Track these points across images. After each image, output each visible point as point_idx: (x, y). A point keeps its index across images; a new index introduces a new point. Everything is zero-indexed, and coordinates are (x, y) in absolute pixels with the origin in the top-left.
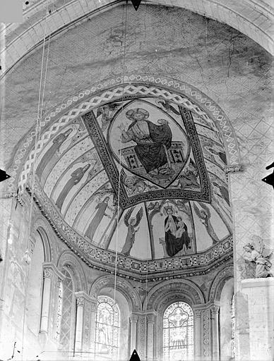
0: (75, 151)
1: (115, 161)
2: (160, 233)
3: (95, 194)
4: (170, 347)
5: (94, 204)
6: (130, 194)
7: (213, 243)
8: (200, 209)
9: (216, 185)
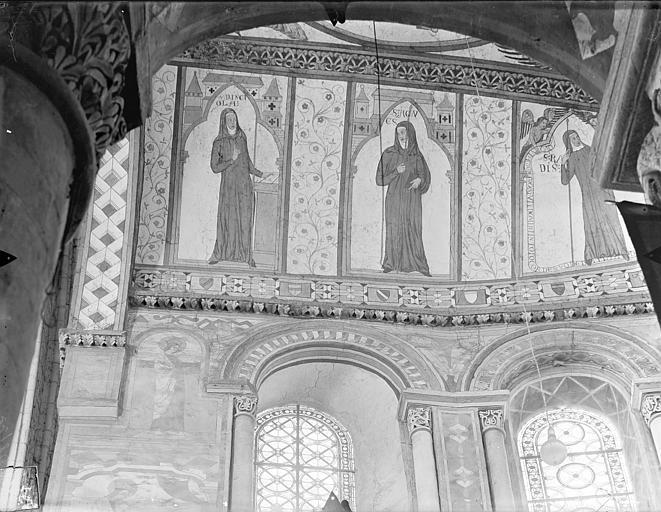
0: (313, 137)
1: (457, 53)
3: (518, 158)
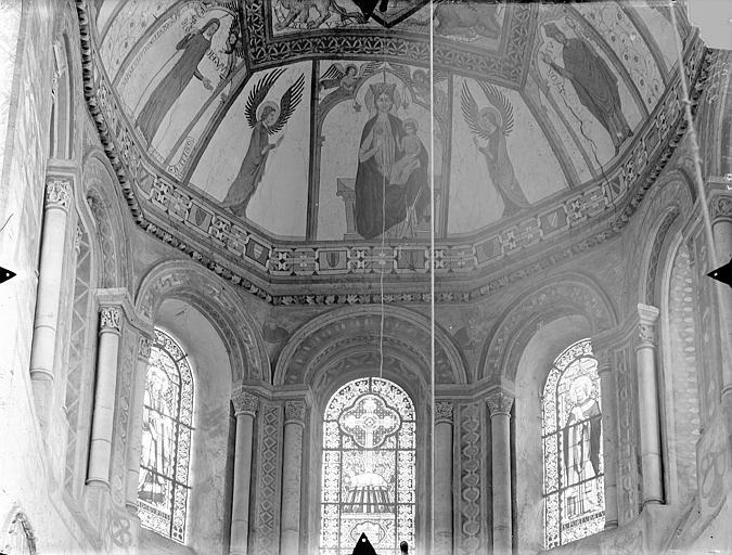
2: (341, 162)
4: (341, 505)
5: (174, 32)
6: (279, 26)
7: (506, 212)
8: (482, 103)
9: (553, 32)
